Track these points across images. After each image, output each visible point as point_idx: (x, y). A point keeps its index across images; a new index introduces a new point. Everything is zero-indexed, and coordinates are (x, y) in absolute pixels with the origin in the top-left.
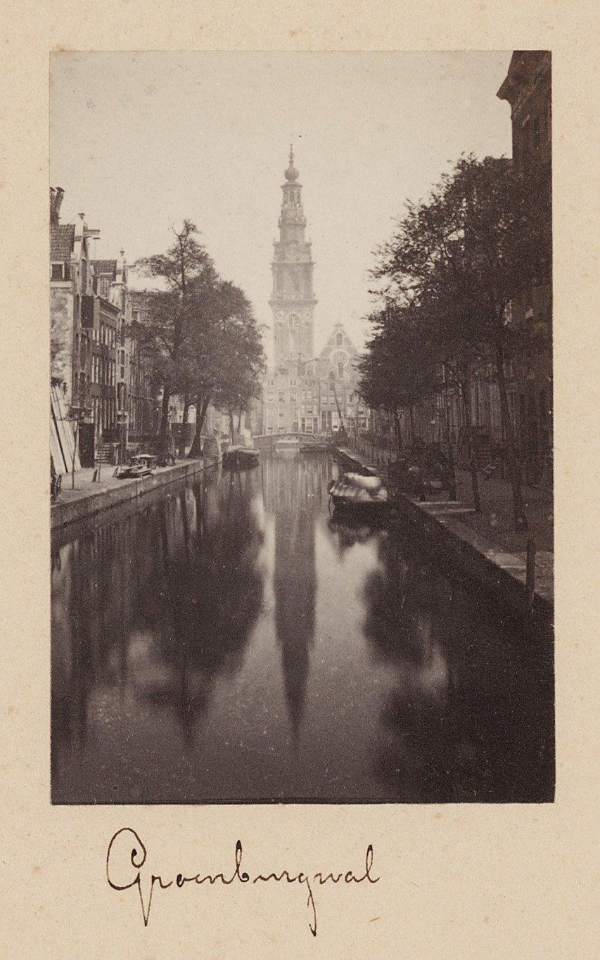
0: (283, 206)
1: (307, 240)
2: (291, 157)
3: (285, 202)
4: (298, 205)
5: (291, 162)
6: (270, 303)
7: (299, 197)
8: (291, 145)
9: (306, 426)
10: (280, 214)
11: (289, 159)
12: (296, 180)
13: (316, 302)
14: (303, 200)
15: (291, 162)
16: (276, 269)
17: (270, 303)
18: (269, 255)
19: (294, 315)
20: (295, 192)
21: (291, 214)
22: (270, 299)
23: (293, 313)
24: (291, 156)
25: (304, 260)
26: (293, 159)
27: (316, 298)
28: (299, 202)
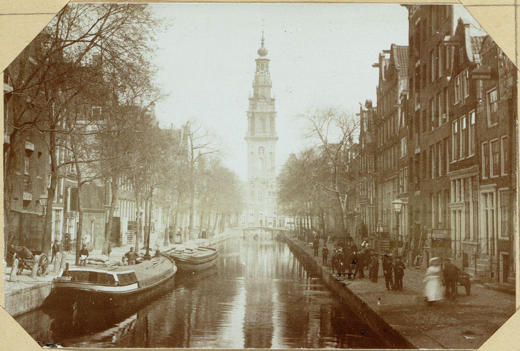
0: (256, 73)
1: (272, 96)
2: (263, 40)
3: (258, 71)
4: (266, 73)
5: (262, 44)
6: (246, 139)
7: (267, 67)
8: (263, 32)
9: (268, 221)
10: (254, 79)
11: (261, 42)
12: (266, 56)
13: (277, 139)
14: (270, 69)
15: (262, 44)
16: (250, 115)
17: (246, 139)
18: (246, 105)
19: (261, 147)
20: (265, 64)
21: (261, 80)
22: (245, 135)
23: (262, 145)
24: (263, 40)
25: (269, 110)
26: (264, 42)
27: (278, 136)
28: (267, 71)
